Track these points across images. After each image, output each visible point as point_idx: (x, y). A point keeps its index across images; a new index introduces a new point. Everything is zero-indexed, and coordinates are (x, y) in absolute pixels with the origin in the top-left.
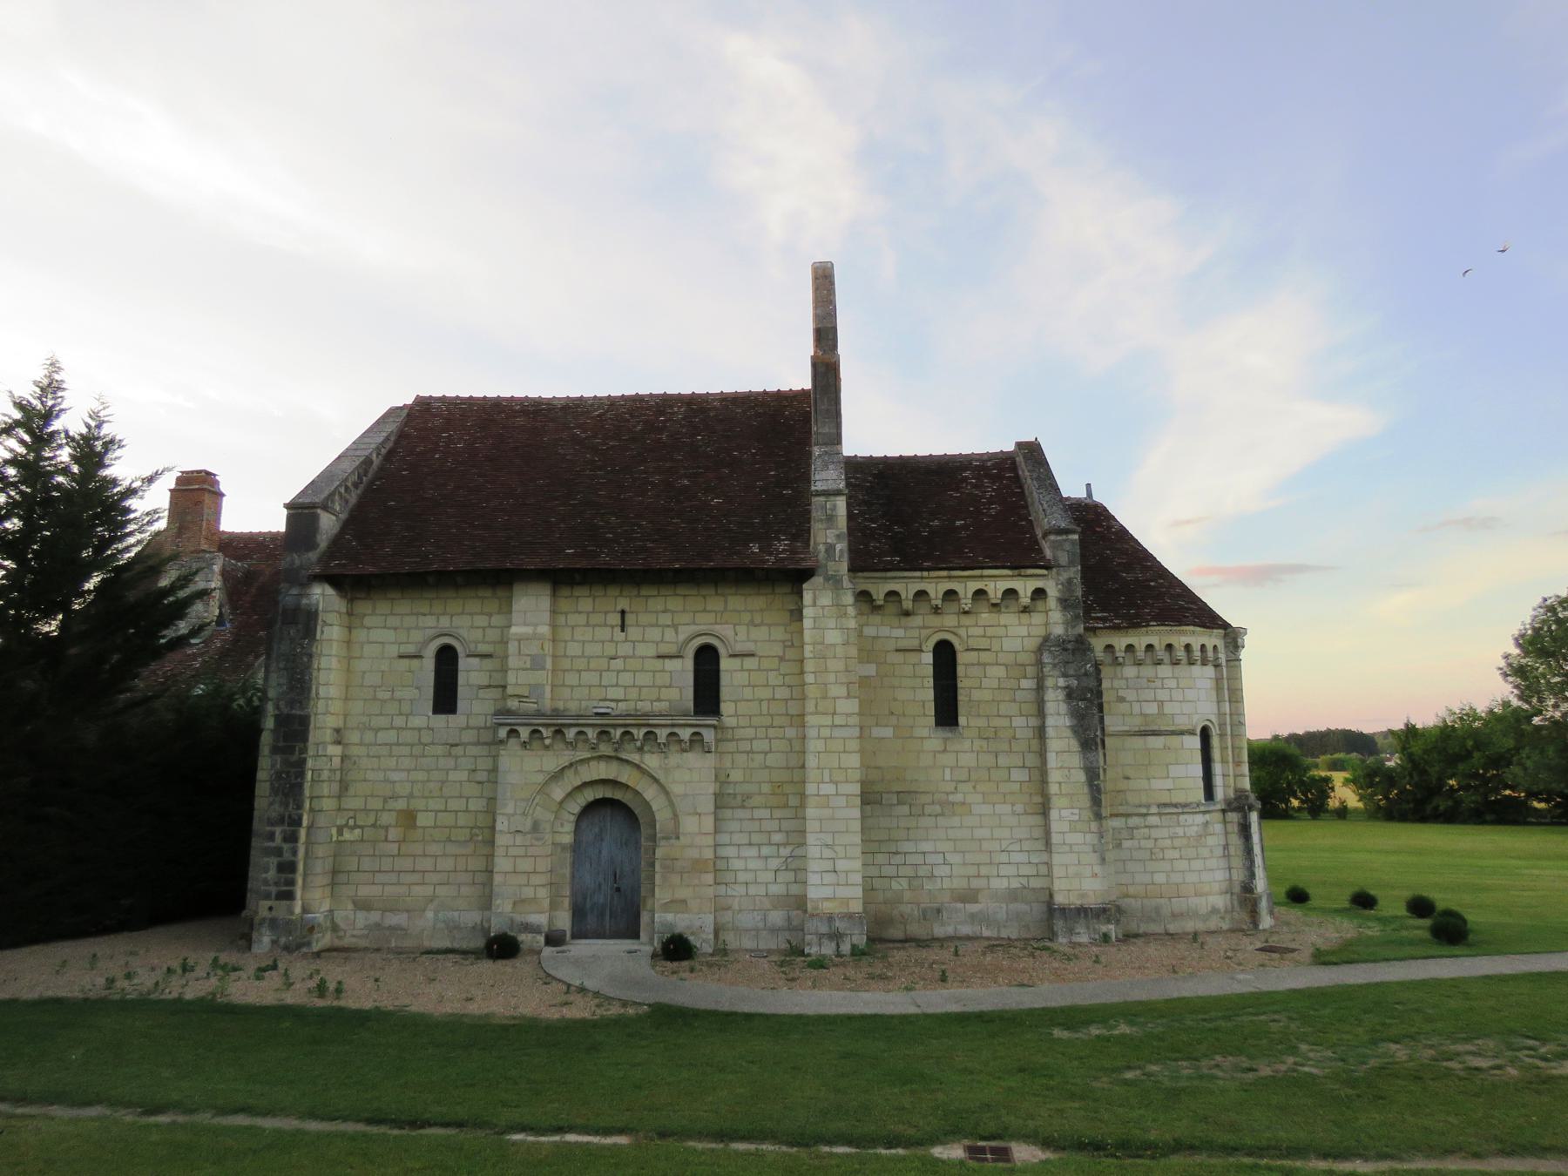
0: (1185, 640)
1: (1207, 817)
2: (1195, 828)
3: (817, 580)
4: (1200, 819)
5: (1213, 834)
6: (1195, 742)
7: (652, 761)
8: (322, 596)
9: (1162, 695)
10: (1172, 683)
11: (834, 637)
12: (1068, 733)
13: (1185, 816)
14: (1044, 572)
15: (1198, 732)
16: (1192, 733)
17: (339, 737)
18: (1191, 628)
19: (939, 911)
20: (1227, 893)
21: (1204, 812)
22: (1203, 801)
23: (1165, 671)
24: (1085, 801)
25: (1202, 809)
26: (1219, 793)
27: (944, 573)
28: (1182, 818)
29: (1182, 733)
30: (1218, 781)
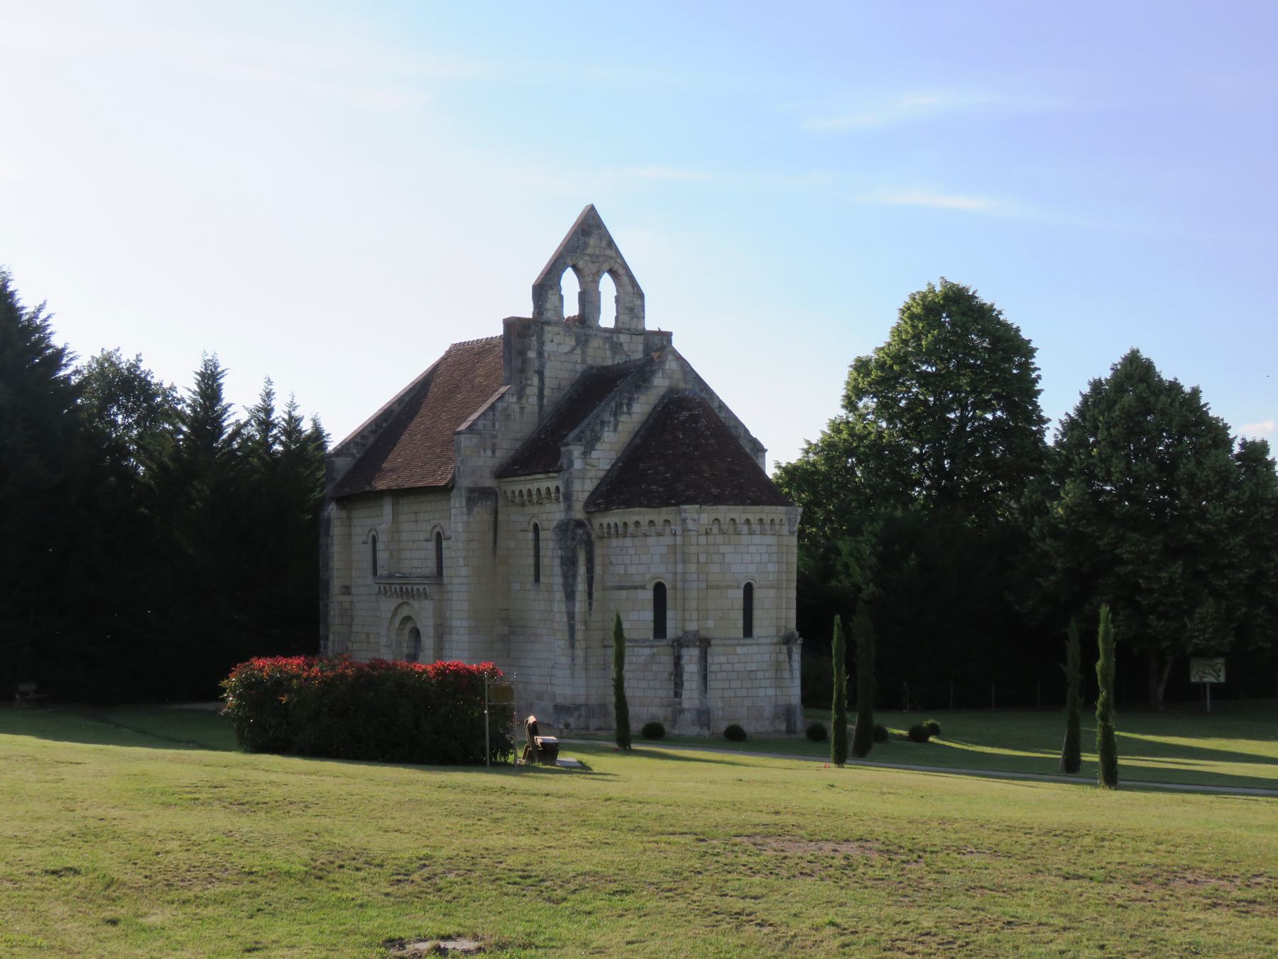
0: (635, 518)
1: (655, 650)
2: (644, 658)
3: (455, 491)
4: (648, 651)
5: (660, 663)
6: (649, 595)
7: (416, 604)
8: (332, 510)
9: (627, 560)
10: (632, 551)
11: (460, 527)
12: (561, 589)
13: (639, 649)
14: (555, 475)
15: (651, 587)
16: (643, 587)
17: (347, 590)
18: (638, 509)
19: (531, 705)
20: (669, 706)
21: (652, 647)
22: (652, 638)
23: (628, 542)
24: (566, 635)
25: (647, 644)
26: (671, 632)
27: (523, 478)
28: (636, 649)
29: (635, 588)
30: (670, 624)
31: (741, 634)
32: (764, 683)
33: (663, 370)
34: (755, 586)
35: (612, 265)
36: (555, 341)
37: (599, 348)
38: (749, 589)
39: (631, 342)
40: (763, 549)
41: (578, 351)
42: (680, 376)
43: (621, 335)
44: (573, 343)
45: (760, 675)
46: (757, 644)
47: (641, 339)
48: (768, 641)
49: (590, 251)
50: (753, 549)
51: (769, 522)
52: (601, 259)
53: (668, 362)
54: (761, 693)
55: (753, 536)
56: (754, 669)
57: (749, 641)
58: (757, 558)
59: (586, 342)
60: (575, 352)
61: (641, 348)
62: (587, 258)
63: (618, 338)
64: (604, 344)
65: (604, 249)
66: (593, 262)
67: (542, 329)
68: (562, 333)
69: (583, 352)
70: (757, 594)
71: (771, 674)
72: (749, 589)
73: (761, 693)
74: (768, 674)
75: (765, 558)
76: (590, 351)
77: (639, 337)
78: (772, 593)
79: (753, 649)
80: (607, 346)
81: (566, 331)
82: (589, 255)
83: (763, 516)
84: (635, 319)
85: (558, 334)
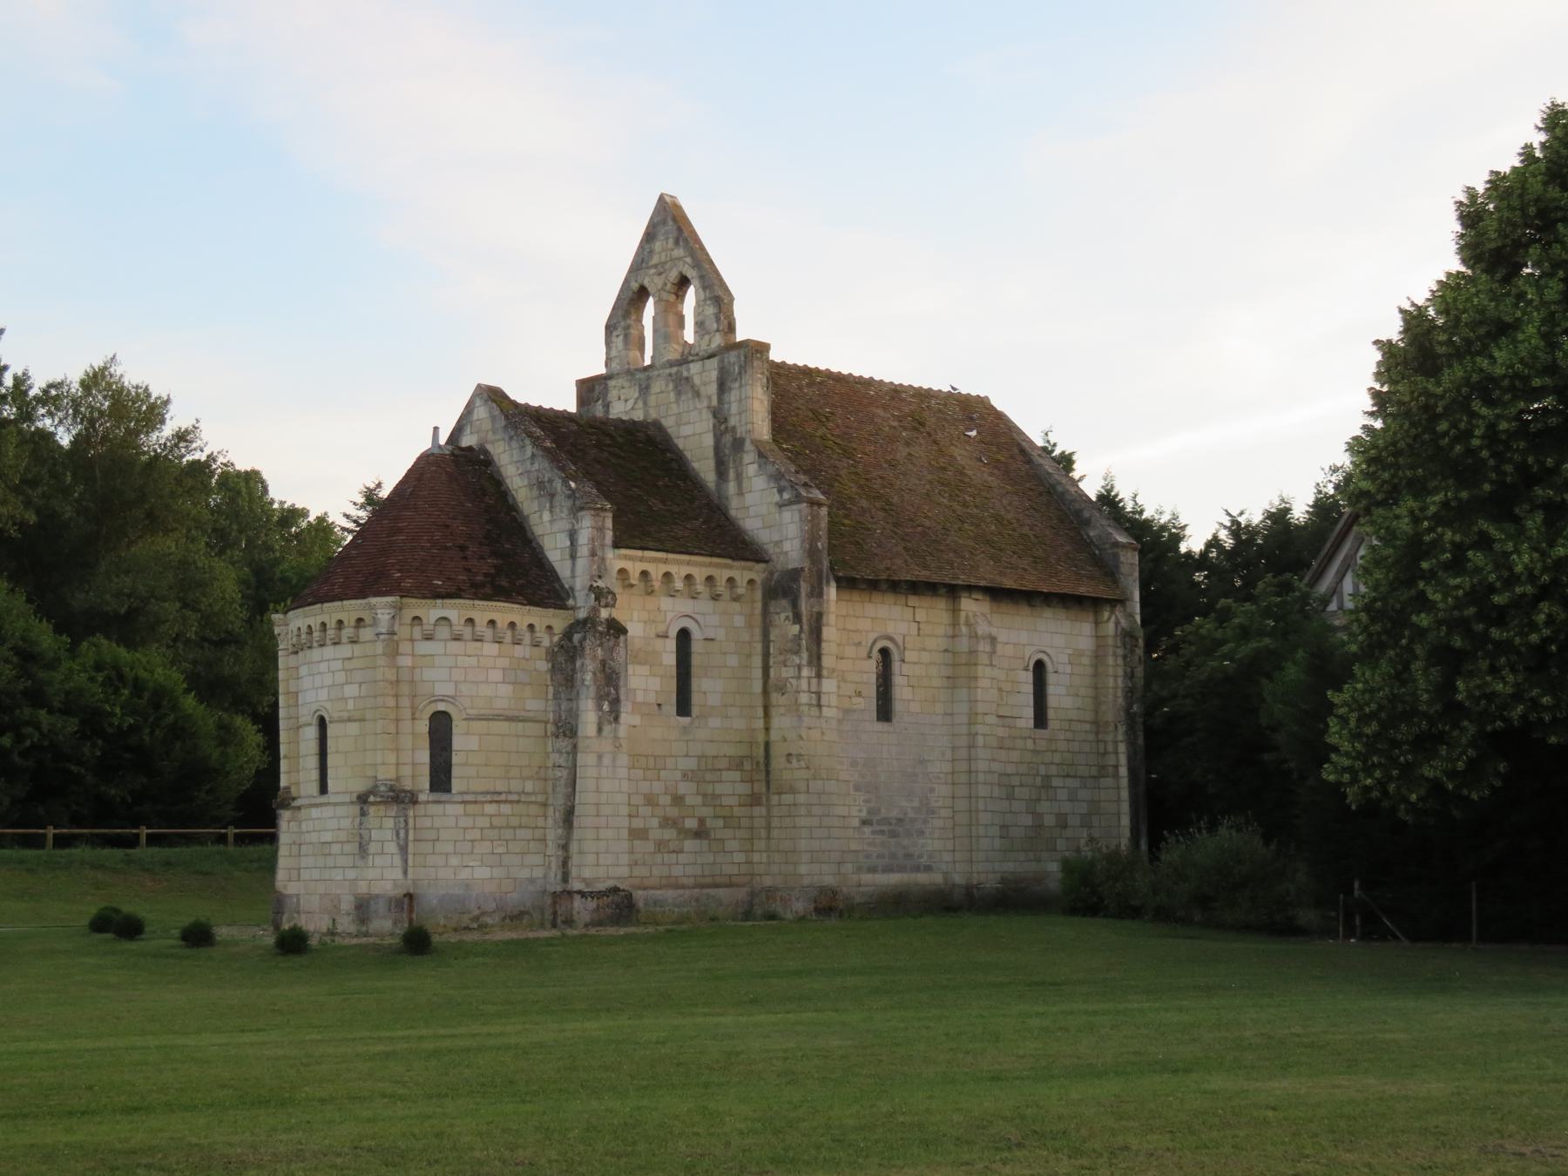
31: (314, 788)
32: (342, 861)
33: (471, 423)
34: (327, 719)
35: (680, 269)
36: (622, 397)
37: (662, 392)
38: (322, 724)
39: (704, 371)
40: (338, 665)
41: (640, 404)
42: (489, 426)
43: (691, 365)
44: (636, 395)
45: (336, 849)
46: (329, 804)
47: (714, 362)
48: (347, 799)
49: (655, 260)
50: (323, 667)
51: (353, 623)
52: (667, 267)
53: (476, 410)
54: (338, 875)
55: (324, 648)
56: (329, 840)
57: (324, 799)
58: (328, 680)
59: (648, 387)
60: (636, 406)
61: (714, 374)
62: (652, 271)
63: (688, 370)
64: (667, 386)
65: (673, 250)
66: (660, 274)
67: (606, 388)
68: (626, 384)
69: (645, 403)
70: (332, 730)
71: (352, 848)
72: (322, 724)
73: (338, 875)
74: (348, 848)
75: (341, 677)
76: (652, 400)
77: (711, 360)
78: (353, 728)
79: (328, 812)
80: (671, 386)
81: (630, 381)
82: (655, 266)
83: (325, 618)
84: (707, 337)
85: (623, 388)
